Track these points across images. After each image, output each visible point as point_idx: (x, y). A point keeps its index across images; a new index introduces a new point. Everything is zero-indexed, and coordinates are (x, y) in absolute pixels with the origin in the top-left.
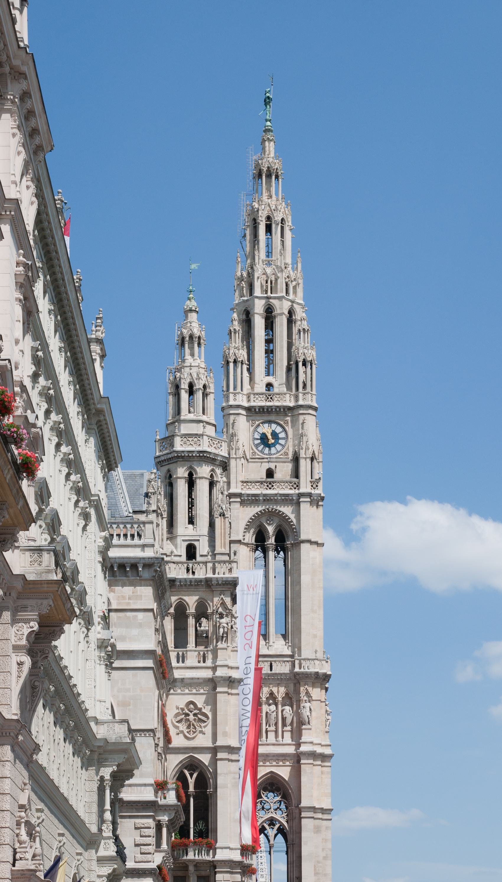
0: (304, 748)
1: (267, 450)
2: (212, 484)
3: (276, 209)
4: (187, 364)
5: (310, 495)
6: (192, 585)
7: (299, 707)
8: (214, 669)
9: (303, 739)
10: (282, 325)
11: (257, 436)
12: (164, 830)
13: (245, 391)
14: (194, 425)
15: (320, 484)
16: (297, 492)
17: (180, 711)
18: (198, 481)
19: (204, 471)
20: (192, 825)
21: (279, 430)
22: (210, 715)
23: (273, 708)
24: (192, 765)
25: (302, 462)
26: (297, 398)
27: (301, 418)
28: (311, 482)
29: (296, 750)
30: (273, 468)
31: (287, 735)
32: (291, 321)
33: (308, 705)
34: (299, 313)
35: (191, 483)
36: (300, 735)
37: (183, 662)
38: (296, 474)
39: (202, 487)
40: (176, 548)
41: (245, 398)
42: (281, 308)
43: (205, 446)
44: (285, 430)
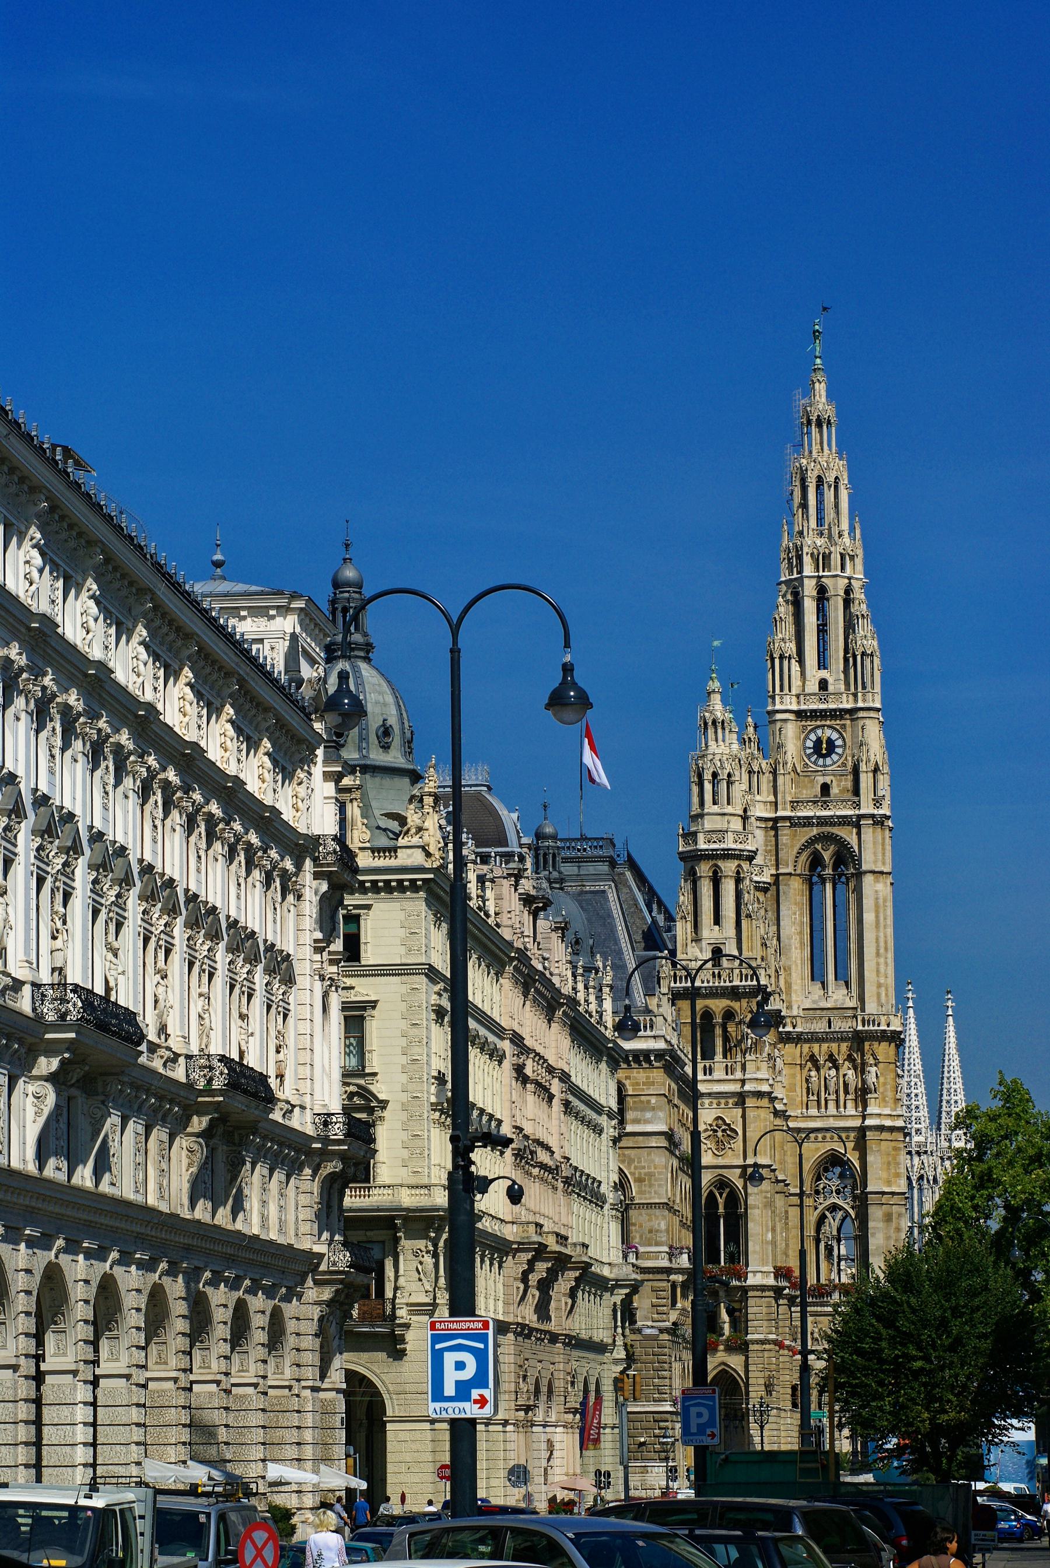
0: (868, 1122)
1: (821, 761)
3: (828, 468)
4: (710, 751)
5: (873, 816)
7: (863, 1072)
8: (743, 1082)
9: (869, 1110)
10: (836, 609)
11: (810, 744)
12: (679, 1290)
13: (794, 692)
15: (887, 802)
16: (857, 812)
18: (723, 880)
19: (729, 867)
20: (722, 1248)
21: (835, 736)
22: (740, 1132)
23: (833, 1072)
24: (722, 1184)
25: (863, 777)
26: (856, 701)
27: (861, 723)
28: (873, 800)
32: (847, 602)
33: (873, 1069)
34: (858, 594)
35: (716, 881)
36: (865, 1106)
38: (856, 792)
39: (728, 888)
40: (701, 951)
41: (794, 699)
42: (836, 589)
43: (730, 844)
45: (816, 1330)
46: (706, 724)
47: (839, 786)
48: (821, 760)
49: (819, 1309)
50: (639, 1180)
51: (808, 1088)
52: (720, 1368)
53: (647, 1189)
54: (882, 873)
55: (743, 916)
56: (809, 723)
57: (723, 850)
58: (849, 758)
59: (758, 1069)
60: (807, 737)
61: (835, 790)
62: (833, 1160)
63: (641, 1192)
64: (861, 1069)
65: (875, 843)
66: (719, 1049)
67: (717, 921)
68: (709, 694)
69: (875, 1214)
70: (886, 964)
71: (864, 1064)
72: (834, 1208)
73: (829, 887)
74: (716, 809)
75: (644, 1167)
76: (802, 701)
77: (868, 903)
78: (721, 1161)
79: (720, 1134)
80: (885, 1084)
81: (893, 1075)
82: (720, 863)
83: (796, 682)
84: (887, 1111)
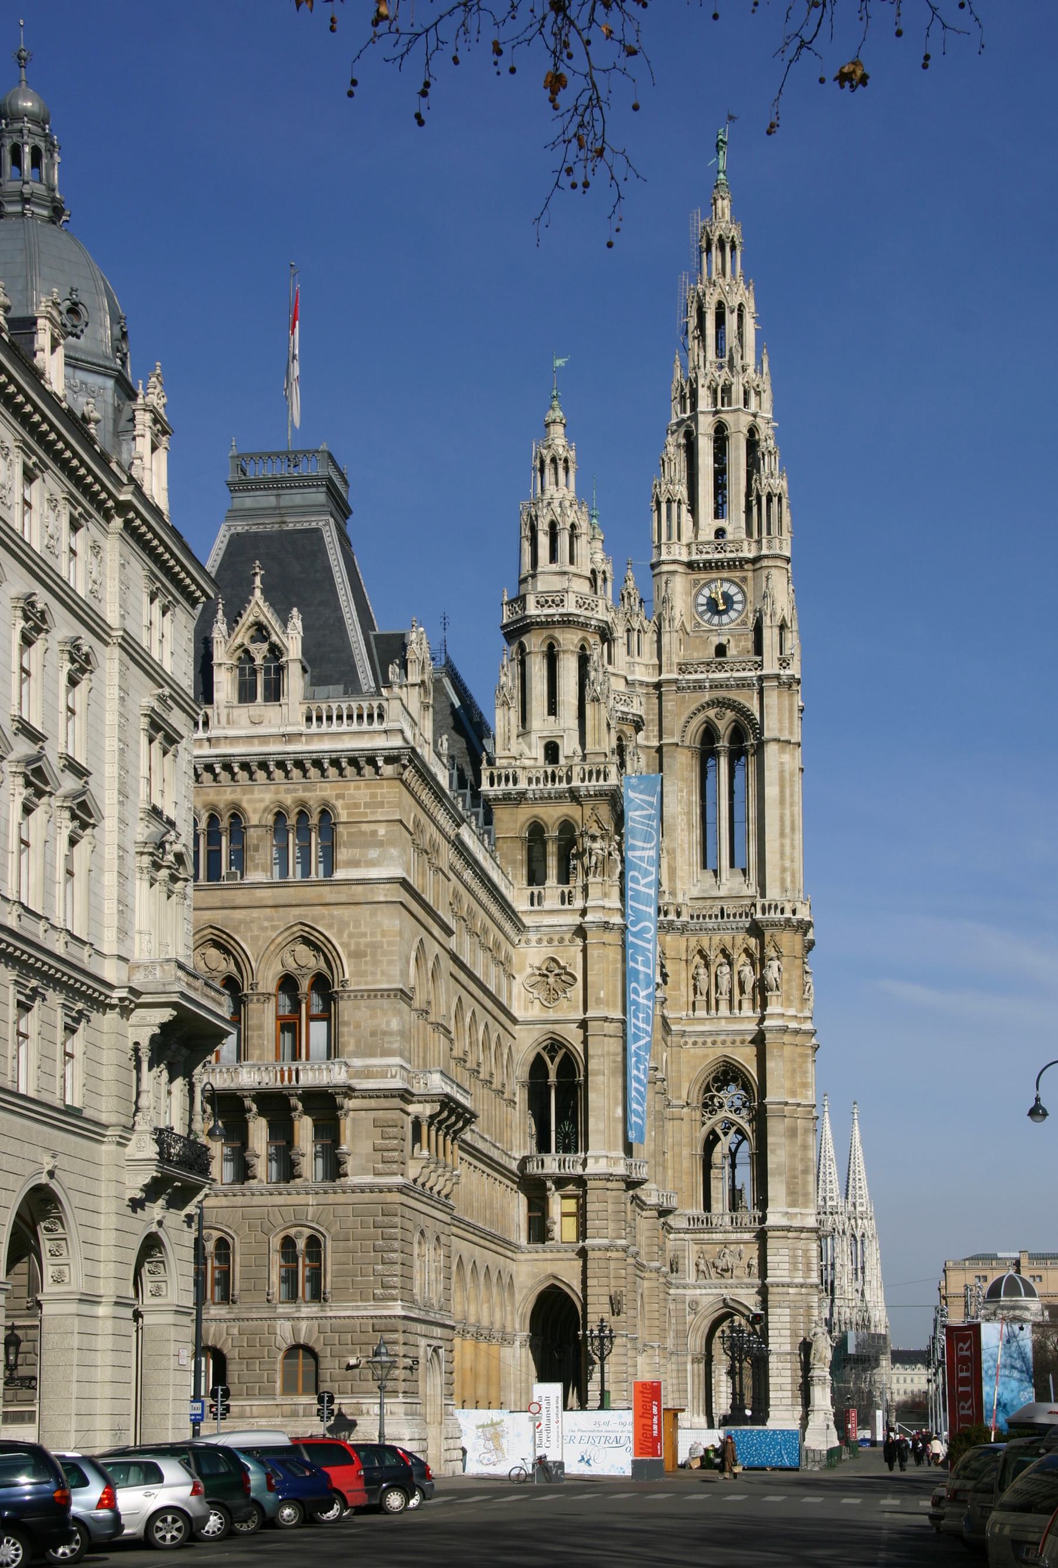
4: (547, 496)
6: (551, 798)
7: (763, 966)
8: (584, 912)
9: (769, 1010)
11: (702, 600)
13: (685, 540)
14: (557, 578)
16: (759, 673)
17: (537, 972)
18: (561, 656)
20: (553, 1128)
21: (733, 590)
24: (554, 1045)
29: (758, 1025)
30: (725, 642)
31: (747, 1005)
36: (764, 1005)
37: (539, 904)
38: (758, 650)
41: (684, 550)
43: (570, 607)
45: (703, 1261)
46: (542, 462)
47: (737, 646)
48: (716, 617)
49: (706, 1236)
50: (357, 955)
51: (695, 986)
52: (547, 1284)
53: (370, 968)
54: (788, 742)
55: (588, 699)
56: (703, 576)
57: (561, 615)
58: (751, 616)
59: (605, 895)
61: (732, 651)
62: (727, 1074)
63: (358, 973)
64: (759, 962)
65: (780, 709)
66: (552, 871)
67: (553, 709)
68: (547, 425)
69: (776, 1131)
70: (793, 846)
71: (762, 960)
72: (729, 1124)
73: (724, 763)
74: (554, 567)
75: (364, 935)
76: (694, 550)
77: (771, 775)
78: (552, 1015)
79: (551, 980)
80: (789, 981)
81: (799, 972)
82: (558, 634)
83: (687, 534)
84: (792, 1012)
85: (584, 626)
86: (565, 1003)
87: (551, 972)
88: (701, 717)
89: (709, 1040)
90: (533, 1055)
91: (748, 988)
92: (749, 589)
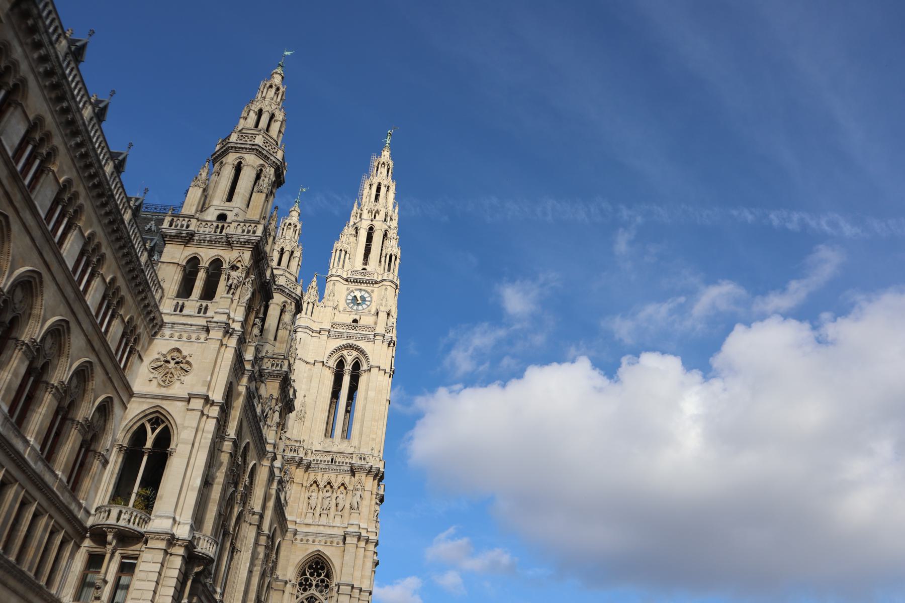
1: (355, 307)
2: (258, 177)
17: (162, 359)
18: (245, 168)
19: (252, 161)
21: (366, 295)
24: (158, 418)
44: (370, 296)
55: (255, 189)
60: (349, 294)
61: (361, 323)
67: (230, 198)
78: (163, 391)
85: (266, 158)
86: (177, 384)
87: (173, 359)
88: (339, 354)
89: (311, 539)
90: (138, 424)
91: (340, 508)
92: (375, 295)
